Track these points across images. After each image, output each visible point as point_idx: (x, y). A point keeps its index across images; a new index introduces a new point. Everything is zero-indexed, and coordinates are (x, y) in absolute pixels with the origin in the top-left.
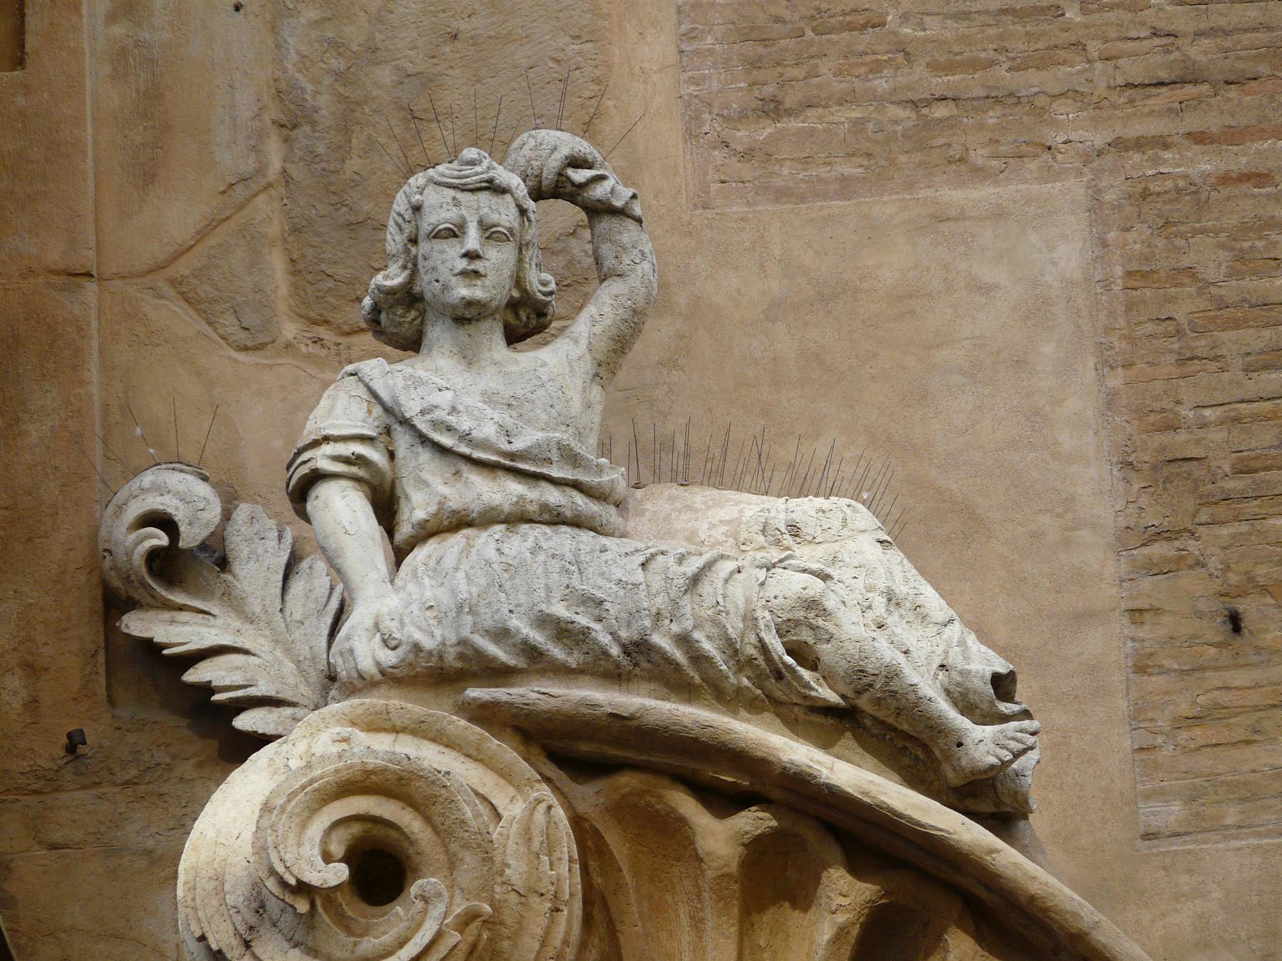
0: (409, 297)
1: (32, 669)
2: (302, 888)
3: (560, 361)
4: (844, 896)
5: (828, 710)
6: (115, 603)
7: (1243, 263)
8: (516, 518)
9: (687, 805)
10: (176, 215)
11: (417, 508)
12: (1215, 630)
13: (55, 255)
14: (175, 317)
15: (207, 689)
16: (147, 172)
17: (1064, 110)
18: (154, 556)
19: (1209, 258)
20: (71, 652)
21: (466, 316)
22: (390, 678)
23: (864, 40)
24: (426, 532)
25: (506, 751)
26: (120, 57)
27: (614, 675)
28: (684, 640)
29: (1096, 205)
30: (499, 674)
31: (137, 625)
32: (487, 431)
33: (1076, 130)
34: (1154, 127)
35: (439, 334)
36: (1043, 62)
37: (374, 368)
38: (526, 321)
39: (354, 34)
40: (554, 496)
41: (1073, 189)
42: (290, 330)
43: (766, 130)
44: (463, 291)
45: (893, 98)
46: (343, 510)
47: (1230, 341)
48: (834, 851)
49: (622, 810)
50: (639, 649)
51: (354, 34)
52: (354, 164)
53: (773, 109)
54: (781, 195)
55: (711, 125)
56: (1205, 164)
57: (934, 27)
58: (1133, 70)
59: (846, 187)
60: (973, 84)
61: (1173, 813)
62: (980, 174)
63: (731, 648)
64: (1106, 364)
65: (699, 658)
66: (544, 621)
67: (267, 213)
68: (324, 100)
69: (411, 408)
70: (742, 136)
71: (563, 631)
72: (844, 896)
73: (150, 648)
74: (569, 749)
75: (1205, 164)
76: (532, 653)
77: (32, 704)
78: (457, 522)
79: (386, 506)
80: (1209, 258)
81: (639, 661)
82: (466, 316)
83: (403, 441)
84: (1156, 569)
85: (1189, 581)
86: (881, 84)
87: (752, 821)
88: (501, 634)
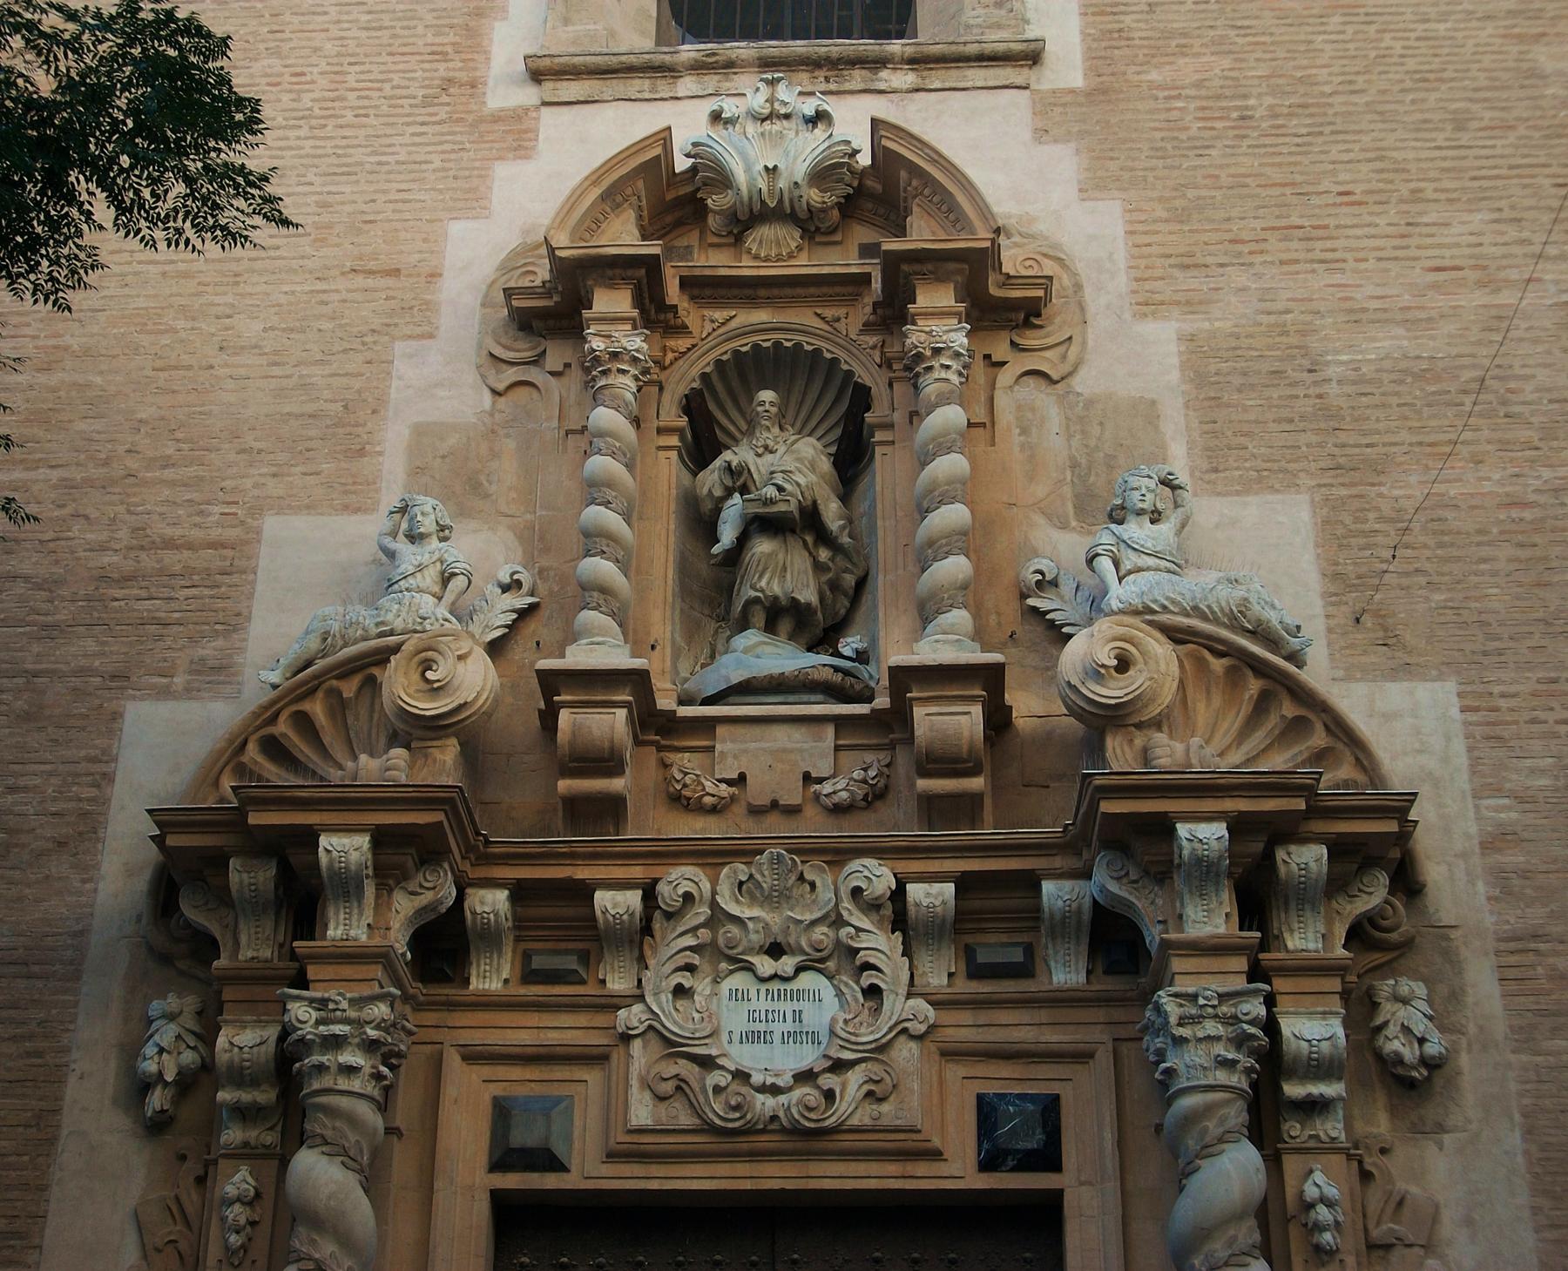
0: (1123, 508)
1: (998, 614)
2: (1103, 666)
3: (1166, 529)
4: (1254, 686)
5: (1249, 631)
6: (1024, 596)
7: (1356, 520)
8: (1157, 569)
9: (1206, 654)
10: (1040, 490)
11: (1127, 565)
12: (1351, 622)
13: (1005, 499)
14: (1040, 520)
15: (1053, 621)
16: (1031, 478)
17: (1302, 475)
18: (1038, 582)
19: (1348, 520)
20: (1011, 609)
21: (1140, 513)
22: (1121, 612)
23: (1242, 453)
24: (1130, 572)
25: (1158, 635)
26: (1022, 447)
27: (1188, 615)
28: (1209, 607)
29: (1313, 501)
30: (1154, 612)
31: (1031, 602)
32: (1149, 545)
33: (1305, 480)
34: (1329, 481)
35: (1131, 518)
36: (1296, 461)
37: (1113, 526)
38: (1156, 517)
39: (1093, 443)
40: (1168, 565)
41: (1304, 498)
42: (1074, 524)
43: (1214, 476)
44: (1141, 505)
45: (1251, 468)
46: (1105, 564)
47: (1353, 541)
48: (1250, 673)
49: (1190, 655)
50: (1195, 608)
51: (1093, 443)
52: (1092, 479)
53: (1216, 470)
54: (1219, 494)
55: (1197, 474)
56: (1344, 492)
57: (1263, 450)
58: (1322, 464)
59: (1238, 493)
60: (1276, 466)
61: (1341, 673)
62: (1277, 491)
63: (1222, 610)
64: (1317, 545)
65: (1213, 612)
66: (1167, 598)
67: (1067, 491)
68: (1083, 461)
69: (1125, 537)
70: (1207, 477)
71: (1173, 602)
72: (1254, 686)
73: (1035, 609)
74: (1176, 635)
75: (1344, 492)
76: (1164, 607)
77: (999, 624)
78: (1139, 570)
79: (1117, 564)
80: (1348, 520)
81: (1196, 611)
82: (1140, 513)
83: (1122, 546)
84: (1333, 604)
85: (1343, 608)
86: (1247, 465)
87: (1225, 661)
88: (1155, 601)
